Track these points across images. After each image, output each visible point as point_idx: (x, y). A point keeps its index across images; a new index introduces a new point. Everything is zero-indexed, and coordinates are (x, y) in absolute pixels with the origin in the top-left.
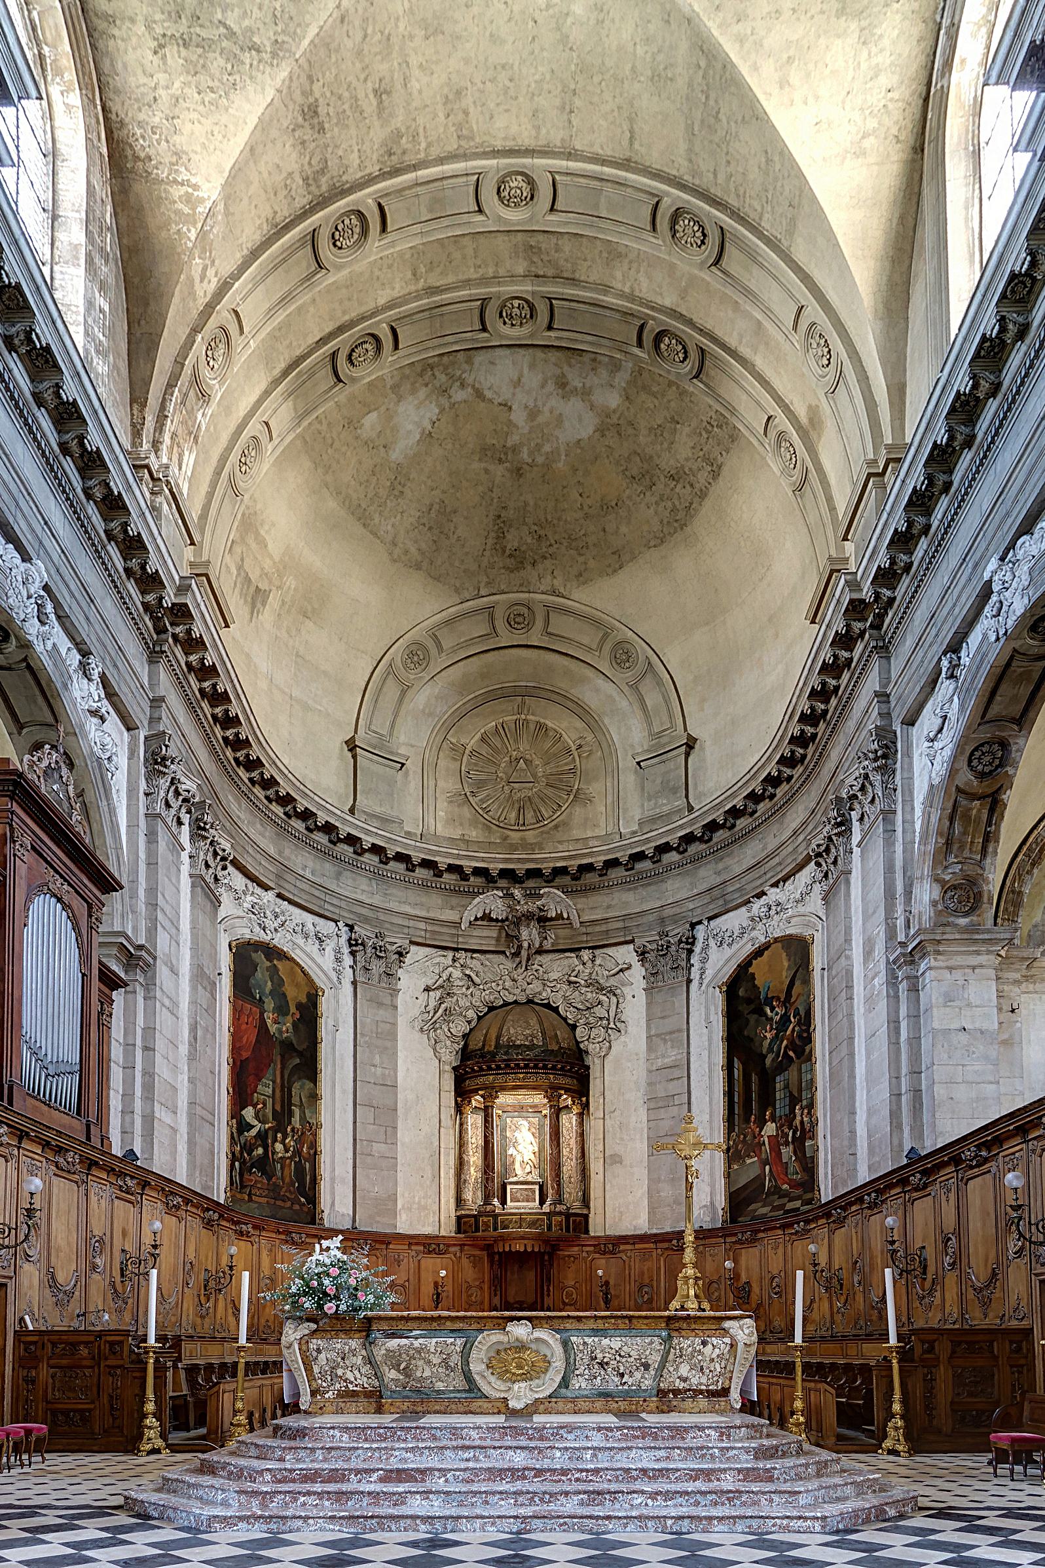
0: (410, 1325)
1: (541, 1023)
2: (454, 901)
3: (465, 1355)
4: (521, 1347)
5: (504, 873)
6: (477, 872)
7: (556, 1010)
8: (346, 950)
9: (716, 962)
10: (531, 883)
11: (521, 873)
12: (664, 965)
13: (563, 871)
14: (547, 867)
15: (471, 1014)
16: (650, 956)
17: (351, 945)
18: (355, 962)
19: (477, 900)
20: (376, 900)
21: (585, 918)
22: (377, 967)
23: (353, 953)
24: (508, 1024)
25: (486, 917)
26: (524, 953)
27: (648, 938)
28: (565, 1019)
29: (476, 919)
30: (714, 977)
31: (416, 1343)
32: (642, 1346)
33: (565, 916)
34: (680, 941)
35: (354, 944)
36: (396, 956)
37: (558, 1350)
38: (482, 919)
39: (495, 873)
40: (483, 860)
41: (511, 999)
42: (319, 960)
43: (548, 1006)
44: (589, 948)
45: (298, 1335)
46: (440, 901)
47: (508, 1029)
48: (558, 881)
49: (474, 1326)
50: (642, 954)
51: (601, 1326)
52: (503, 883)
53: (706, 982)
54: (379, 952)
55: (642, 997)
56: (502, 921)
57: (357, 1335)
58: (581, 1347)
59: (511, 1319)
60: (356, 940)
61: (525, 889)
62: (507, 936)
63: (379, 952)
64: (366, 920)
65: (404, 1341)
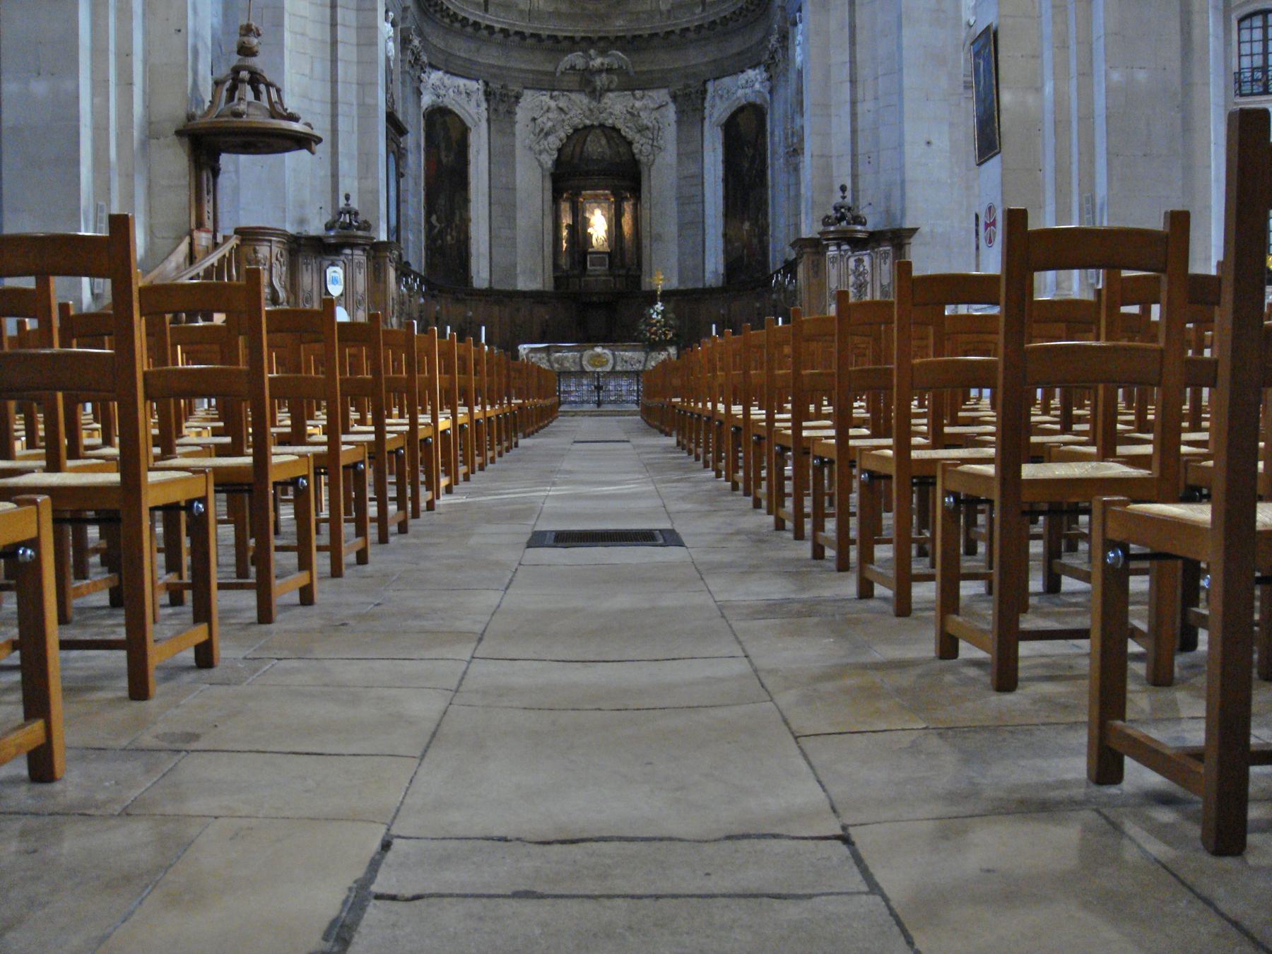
1: (608, 142)
3: (581, 357)
4: (599, 355)
5: (583, 38)
7: (619, 131)
8: (482, 98)
9: (717, 110)
10: (602, 44)
15: (563, 135)
16: (679, 99)
20: (501, 63)
21: (638, 69)
22: (502, 108)
23: (487, 100)
25: (573, 68)
28: (625, 138)
32: (640, 355)
35: (488, 95)
37: (610, 356)
39: (578, 39)
41: (588, 122)
42: (467, 108)
43: (613, 128)
50: (674, 98)
52: (584, 45)
54: (504, 97)
55: (674, 127)
62: (586, 82)
63: (504, 97)
64: (494, 76)
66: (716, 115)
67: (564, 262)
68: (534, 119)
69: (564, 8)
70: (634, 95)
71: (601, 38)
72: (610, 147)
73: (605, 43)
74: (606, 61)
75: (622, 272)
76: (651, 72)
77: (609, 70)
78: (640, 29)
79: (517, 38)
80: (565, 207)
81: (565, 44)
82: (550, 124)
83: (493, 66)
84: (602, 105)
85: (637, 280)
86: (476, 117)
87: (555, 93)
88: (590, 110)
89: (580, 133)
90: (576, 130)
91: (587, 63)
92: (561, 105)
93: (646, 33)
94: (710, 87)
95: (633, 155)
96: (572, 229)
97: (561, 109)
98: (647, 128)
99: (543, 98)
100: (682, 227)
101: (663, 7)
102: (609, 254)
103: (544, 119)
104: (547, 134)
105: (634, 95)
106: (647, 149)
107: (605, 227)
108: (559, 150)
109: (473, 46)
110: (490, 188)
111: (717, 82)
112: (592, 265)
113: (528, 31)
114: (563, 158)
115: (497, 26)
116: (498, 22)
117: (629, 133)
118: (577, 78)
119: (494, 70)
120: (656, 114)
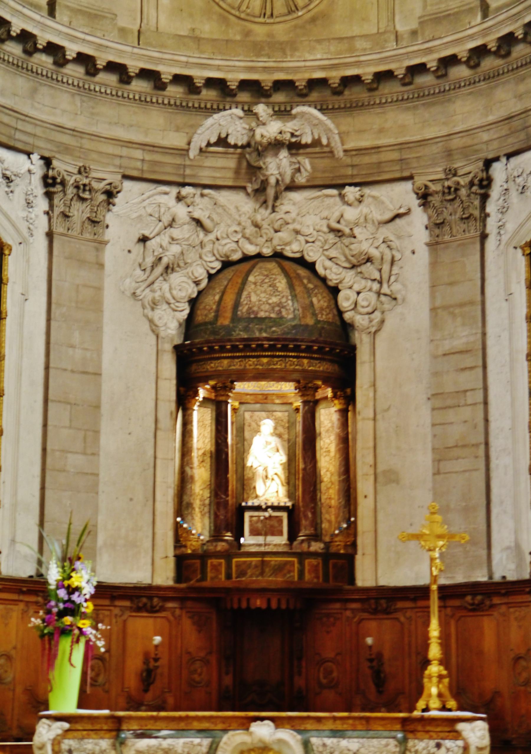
0: (159, 725)
1: (291, 286)
2: (181, 118)
5: (246, 85)
6: (210, 82)
7: (311, 267)
8: (39, 190)
10: (279, 97)
11: (267, 85)
12: (452, 213)
13: (323, 82)
14: (301, 78)
15: (201, 273)
16: (435, 200)
17: (46, 184)
18: (51, 206)
19: (210, 121)
20: (79, 124)
22: (79, 212)
23: (49, 195)
24: (249, 288)
25: (222, 142)
26: (271, 192)
27: (431, 175)
28: (324, 280)
29: (209, 145)
30: (516, 232)
31: (166, 743)
33: (324, 141)
34: (471, 184)
35: (50, 183)
36: (103, 197)
38: (216, 144)
39: (233, 86)
40: (219, 68)
41: (251, 250)
43: (301, 261)
44: (356, 185)
45: (52, 735)
46: (161, 121)
47: (249, 296)
48: (314, 96)
49: (220, 726)
50: (424, 197)
51: (340, 727)
52: (244, 97)
53: (505, 238)
55: (423, 254)
56: (243, 147)
57: (108, 735)
58: (321, 749)
59: (256, 719)
60: (54, 178)
61: (272, 105)
64: (67, 149)
65: (152, 742)
66: (510, 227)
67: (200, 527)
68: (144, 240)
69: (208, 29)
70: (342, 196)
71: (279, 85)
72: (294, 297)
73: (288, 91)
74: (290, 126)
75: (316, 547)
76: (377, 149)
77: (295, 147)
78: (358, 64)
79: (112, 79)
80: (201, 418)
81: (209, 95)
82: (175, 249)
83: (61, 128)
84: (279, 215)
85: (342, 562)
86: (23, 227)
87: (187, 191)
88: (257, 225)
89: (235, 267)
90: (227, 264)
91: (252, 130)
92: (196, 215)
93: (367, 73)
94: (498, 171)
95: (340, 313)
96: (219, 457)
97: (198, 222)
98: (369, 260)
99: (163, 199)
100: (441, 455)
101: (403, 27)
102: (291, 512)
103: (164, 239)
104: (168, 269)
105: (342, 196)
106: (367, 299)
107: (282, 457)
108: (193, 303)
109: (22, 83)
110: (47, 368)
111: (514, 161)
112: (255, 532)
113: (134, 65)
114: (200, 318)
115: (72, 49)
116: (73, 39)
117: (333, 273)
118: (231, 163)
119: (66, 139)
120: (386, 232)
